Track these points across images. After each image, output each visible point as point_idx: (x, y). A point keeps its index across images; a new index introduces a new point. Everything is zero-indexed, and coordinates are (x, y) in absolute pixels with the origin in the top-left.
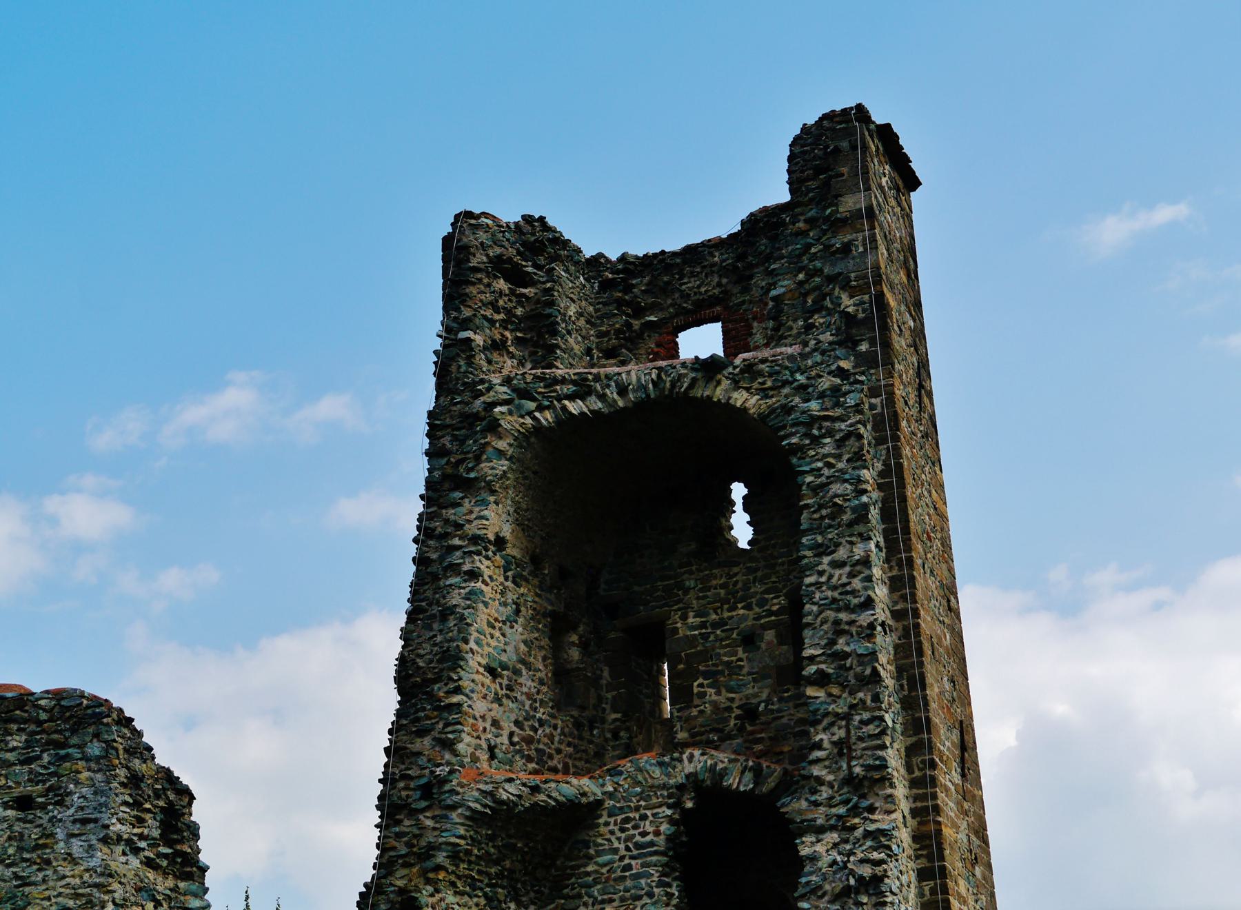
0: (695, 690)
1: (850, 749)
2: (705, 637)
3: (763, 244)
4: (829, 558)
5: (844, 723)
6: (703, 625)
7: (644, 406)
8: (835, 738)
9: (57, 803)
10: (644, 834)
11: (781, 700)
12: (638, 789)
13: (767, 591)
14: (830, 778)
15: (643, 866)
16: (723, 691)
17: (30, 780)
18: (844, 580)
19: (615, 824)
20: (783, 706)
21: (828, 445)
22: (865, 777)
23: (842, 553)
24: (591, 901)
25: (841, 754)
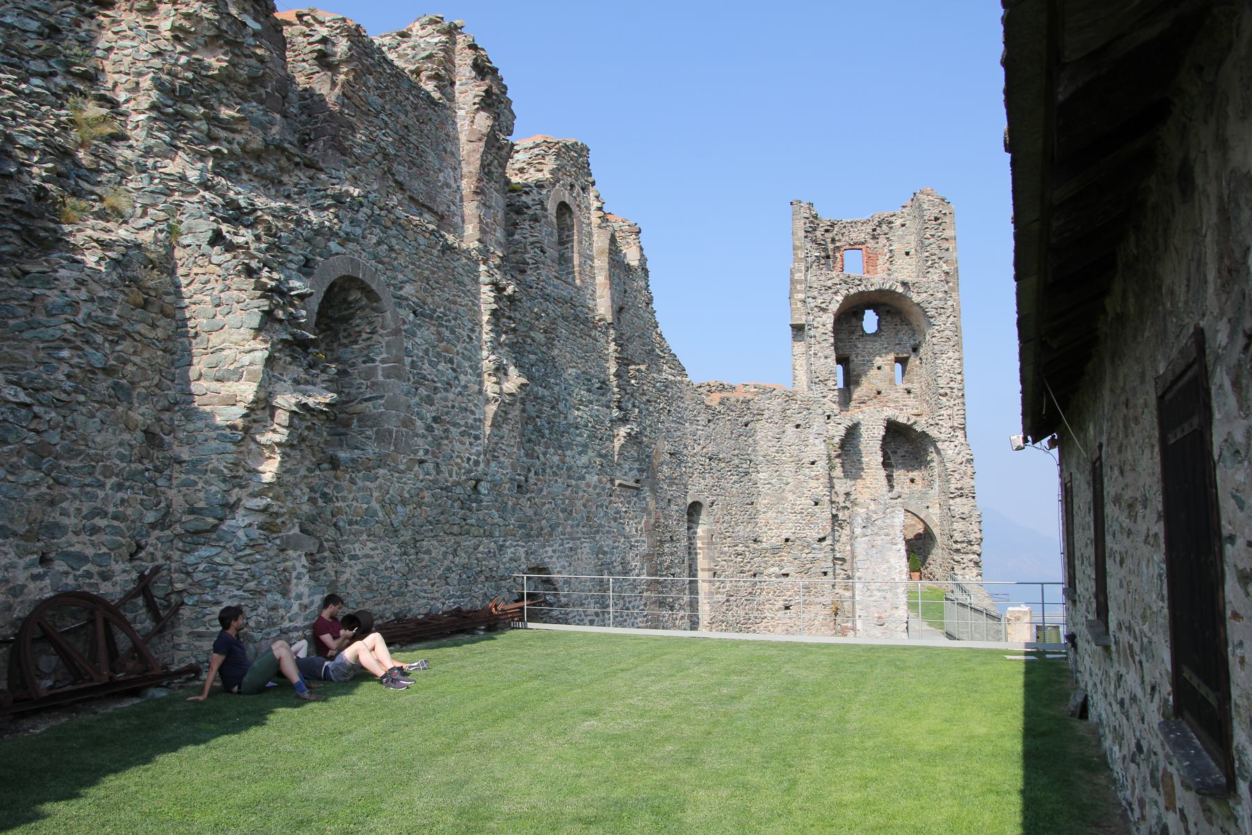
3: (884, 226)
21: (944, 317)
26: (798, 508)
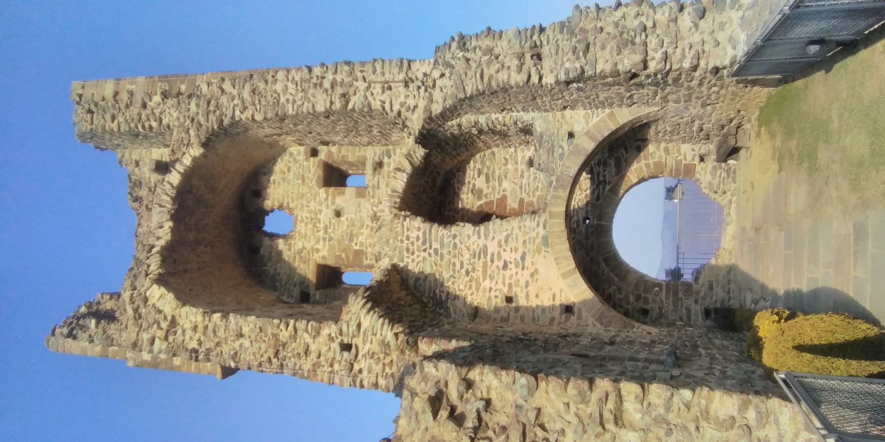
0: (358, 248)
2: (331, 239)
4: (281, 96)
5: (372, 85)
6: (324, 239)
8: (380, 91)
10: (418, 238)
11: (373, 197)
13: (315, 200)
14: (402, 96)
16: (362, 231)
19: (408, 257)
20: (376, 196)
21: (224, 100)
22: (406, 73)
24: (452, 280)
25: (390, 88)
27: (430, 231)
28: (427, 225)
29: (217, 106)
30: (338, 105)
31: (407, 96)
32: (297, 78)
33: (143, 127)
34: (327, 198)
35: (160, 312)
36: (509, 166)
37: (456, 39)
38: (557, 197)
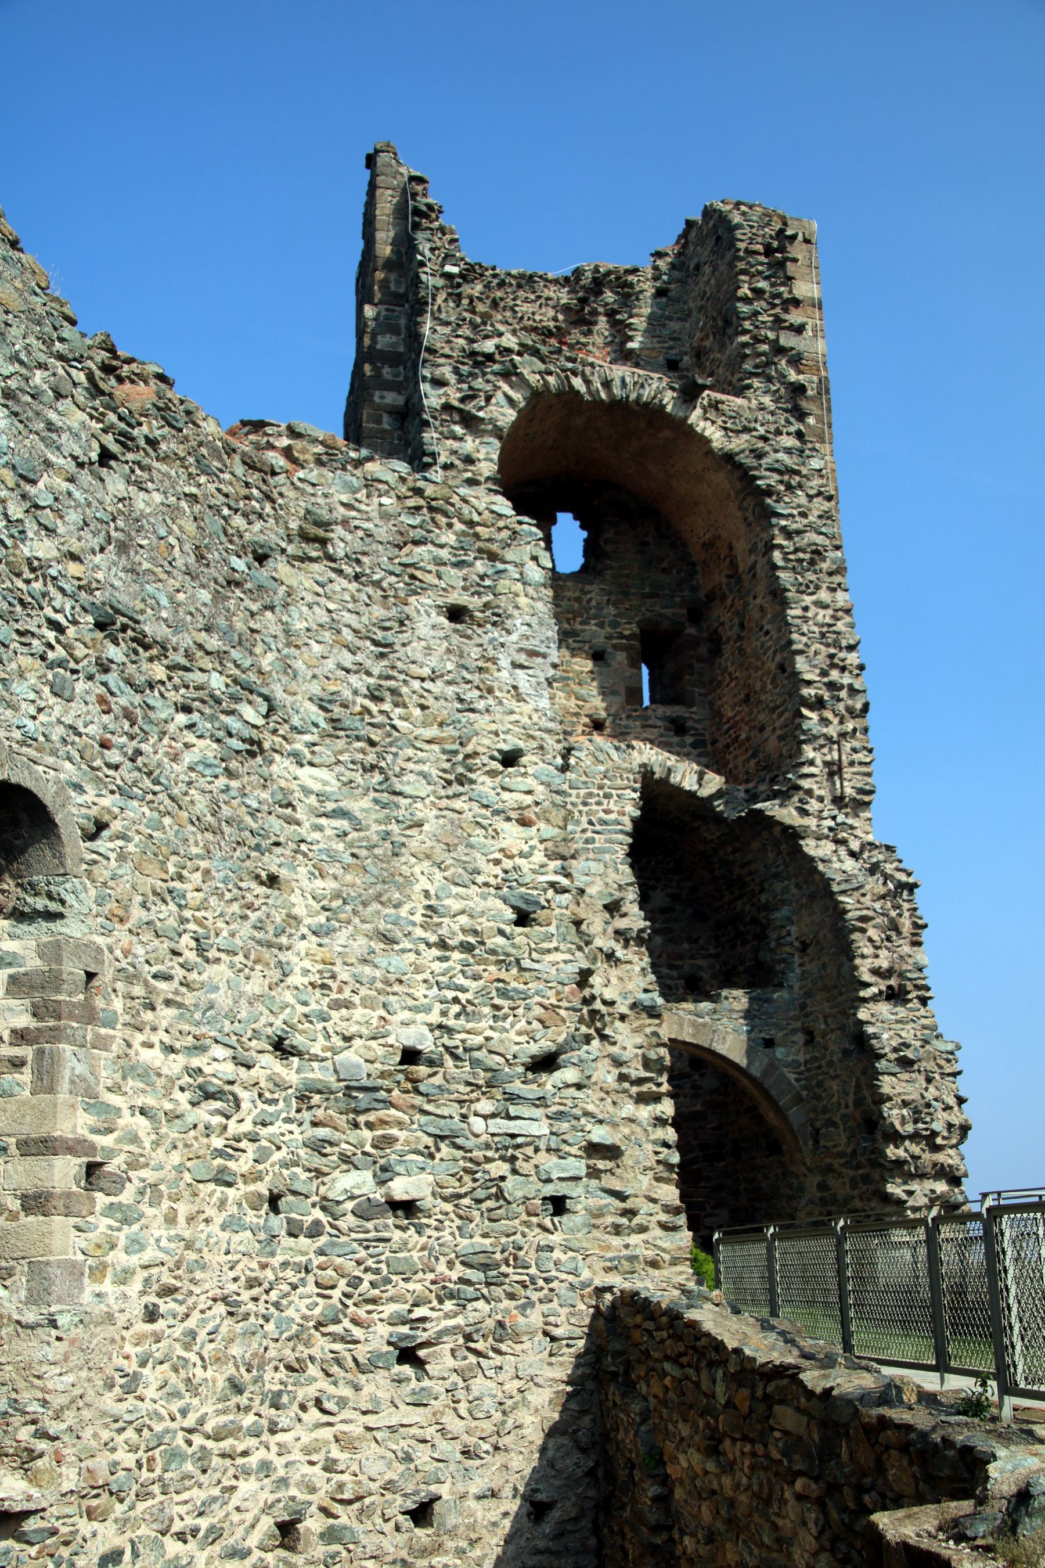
1: (840, 769)
3: (609, 296)
4: (814, 598)
7: (619, 408)
8: (828, 758)
9: (494, 624)
11: (629, 717)
12: (602, 768)
15: (607, 841)
17: (464, 589)
18: (828, 620)
23: (824, 595)
26: (453, 928)
27: (622, 832)
28: (629, 827)
29: (789, 487)
30: (806, 692)
31: (821, 799)
32: (840, 626)
33: (745, 345)
34: (622, 636)
35: (488, 399)
36: (686, 946)
37: (911, 880)
38: (681, 1025)
